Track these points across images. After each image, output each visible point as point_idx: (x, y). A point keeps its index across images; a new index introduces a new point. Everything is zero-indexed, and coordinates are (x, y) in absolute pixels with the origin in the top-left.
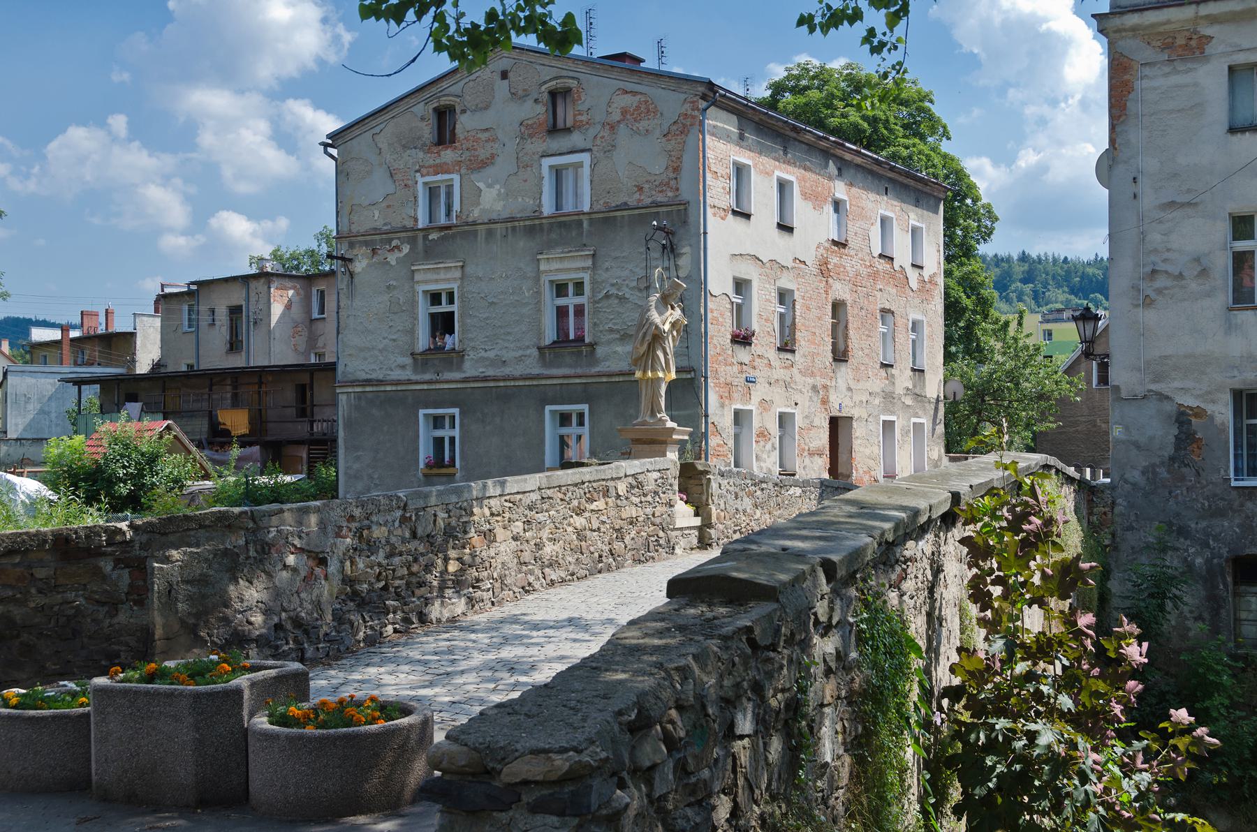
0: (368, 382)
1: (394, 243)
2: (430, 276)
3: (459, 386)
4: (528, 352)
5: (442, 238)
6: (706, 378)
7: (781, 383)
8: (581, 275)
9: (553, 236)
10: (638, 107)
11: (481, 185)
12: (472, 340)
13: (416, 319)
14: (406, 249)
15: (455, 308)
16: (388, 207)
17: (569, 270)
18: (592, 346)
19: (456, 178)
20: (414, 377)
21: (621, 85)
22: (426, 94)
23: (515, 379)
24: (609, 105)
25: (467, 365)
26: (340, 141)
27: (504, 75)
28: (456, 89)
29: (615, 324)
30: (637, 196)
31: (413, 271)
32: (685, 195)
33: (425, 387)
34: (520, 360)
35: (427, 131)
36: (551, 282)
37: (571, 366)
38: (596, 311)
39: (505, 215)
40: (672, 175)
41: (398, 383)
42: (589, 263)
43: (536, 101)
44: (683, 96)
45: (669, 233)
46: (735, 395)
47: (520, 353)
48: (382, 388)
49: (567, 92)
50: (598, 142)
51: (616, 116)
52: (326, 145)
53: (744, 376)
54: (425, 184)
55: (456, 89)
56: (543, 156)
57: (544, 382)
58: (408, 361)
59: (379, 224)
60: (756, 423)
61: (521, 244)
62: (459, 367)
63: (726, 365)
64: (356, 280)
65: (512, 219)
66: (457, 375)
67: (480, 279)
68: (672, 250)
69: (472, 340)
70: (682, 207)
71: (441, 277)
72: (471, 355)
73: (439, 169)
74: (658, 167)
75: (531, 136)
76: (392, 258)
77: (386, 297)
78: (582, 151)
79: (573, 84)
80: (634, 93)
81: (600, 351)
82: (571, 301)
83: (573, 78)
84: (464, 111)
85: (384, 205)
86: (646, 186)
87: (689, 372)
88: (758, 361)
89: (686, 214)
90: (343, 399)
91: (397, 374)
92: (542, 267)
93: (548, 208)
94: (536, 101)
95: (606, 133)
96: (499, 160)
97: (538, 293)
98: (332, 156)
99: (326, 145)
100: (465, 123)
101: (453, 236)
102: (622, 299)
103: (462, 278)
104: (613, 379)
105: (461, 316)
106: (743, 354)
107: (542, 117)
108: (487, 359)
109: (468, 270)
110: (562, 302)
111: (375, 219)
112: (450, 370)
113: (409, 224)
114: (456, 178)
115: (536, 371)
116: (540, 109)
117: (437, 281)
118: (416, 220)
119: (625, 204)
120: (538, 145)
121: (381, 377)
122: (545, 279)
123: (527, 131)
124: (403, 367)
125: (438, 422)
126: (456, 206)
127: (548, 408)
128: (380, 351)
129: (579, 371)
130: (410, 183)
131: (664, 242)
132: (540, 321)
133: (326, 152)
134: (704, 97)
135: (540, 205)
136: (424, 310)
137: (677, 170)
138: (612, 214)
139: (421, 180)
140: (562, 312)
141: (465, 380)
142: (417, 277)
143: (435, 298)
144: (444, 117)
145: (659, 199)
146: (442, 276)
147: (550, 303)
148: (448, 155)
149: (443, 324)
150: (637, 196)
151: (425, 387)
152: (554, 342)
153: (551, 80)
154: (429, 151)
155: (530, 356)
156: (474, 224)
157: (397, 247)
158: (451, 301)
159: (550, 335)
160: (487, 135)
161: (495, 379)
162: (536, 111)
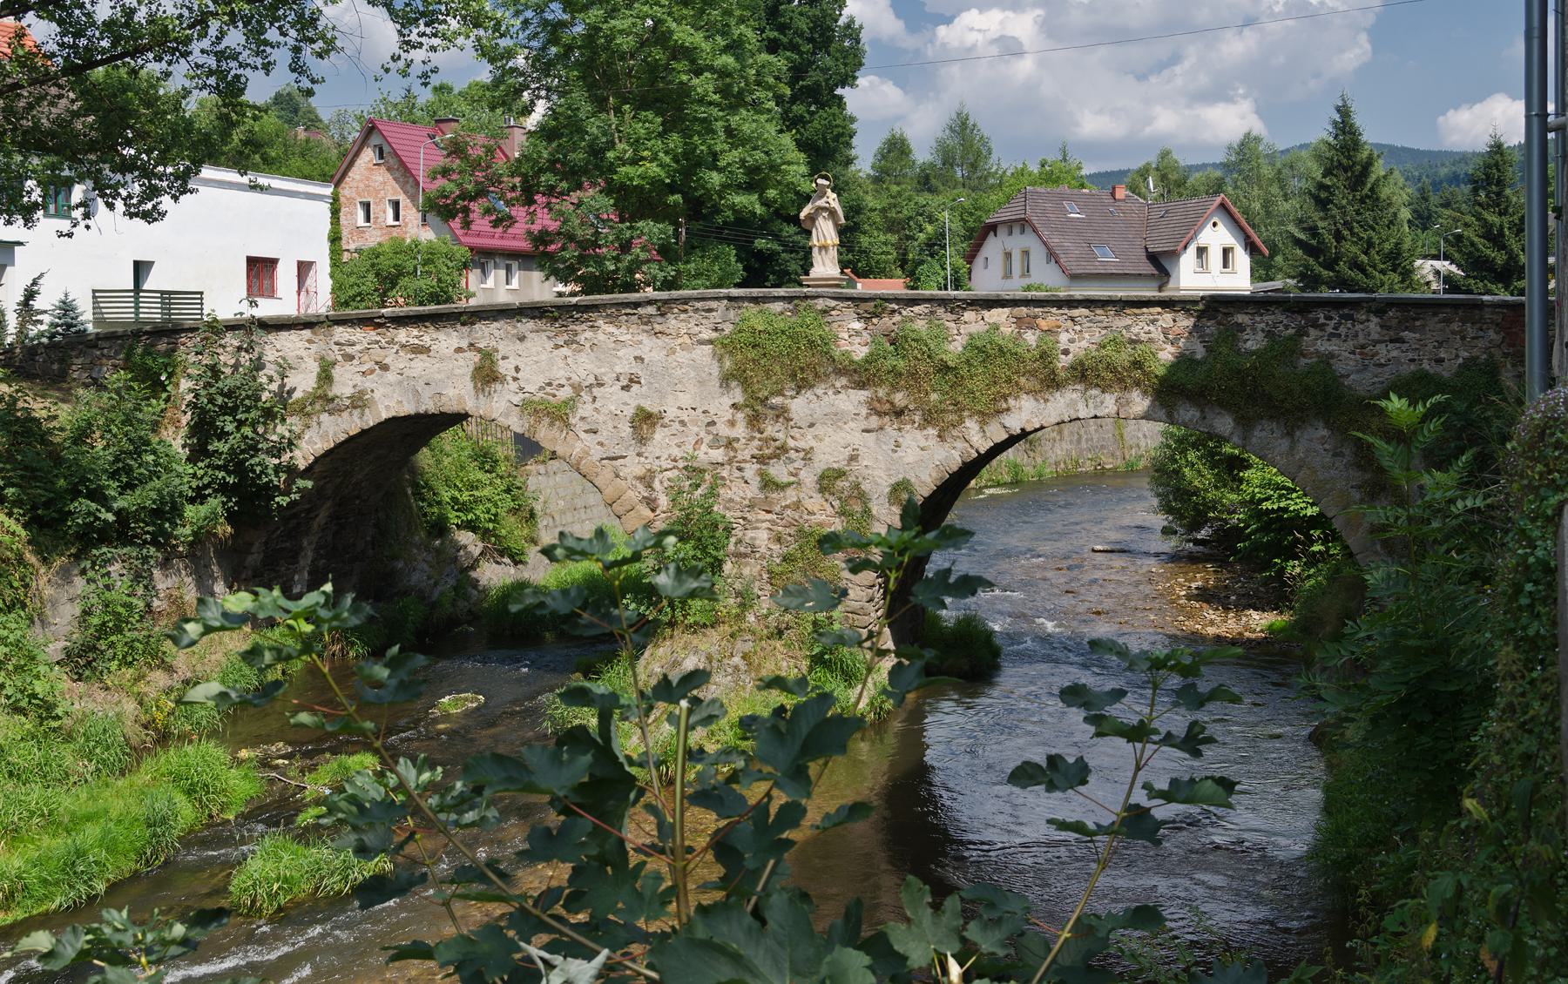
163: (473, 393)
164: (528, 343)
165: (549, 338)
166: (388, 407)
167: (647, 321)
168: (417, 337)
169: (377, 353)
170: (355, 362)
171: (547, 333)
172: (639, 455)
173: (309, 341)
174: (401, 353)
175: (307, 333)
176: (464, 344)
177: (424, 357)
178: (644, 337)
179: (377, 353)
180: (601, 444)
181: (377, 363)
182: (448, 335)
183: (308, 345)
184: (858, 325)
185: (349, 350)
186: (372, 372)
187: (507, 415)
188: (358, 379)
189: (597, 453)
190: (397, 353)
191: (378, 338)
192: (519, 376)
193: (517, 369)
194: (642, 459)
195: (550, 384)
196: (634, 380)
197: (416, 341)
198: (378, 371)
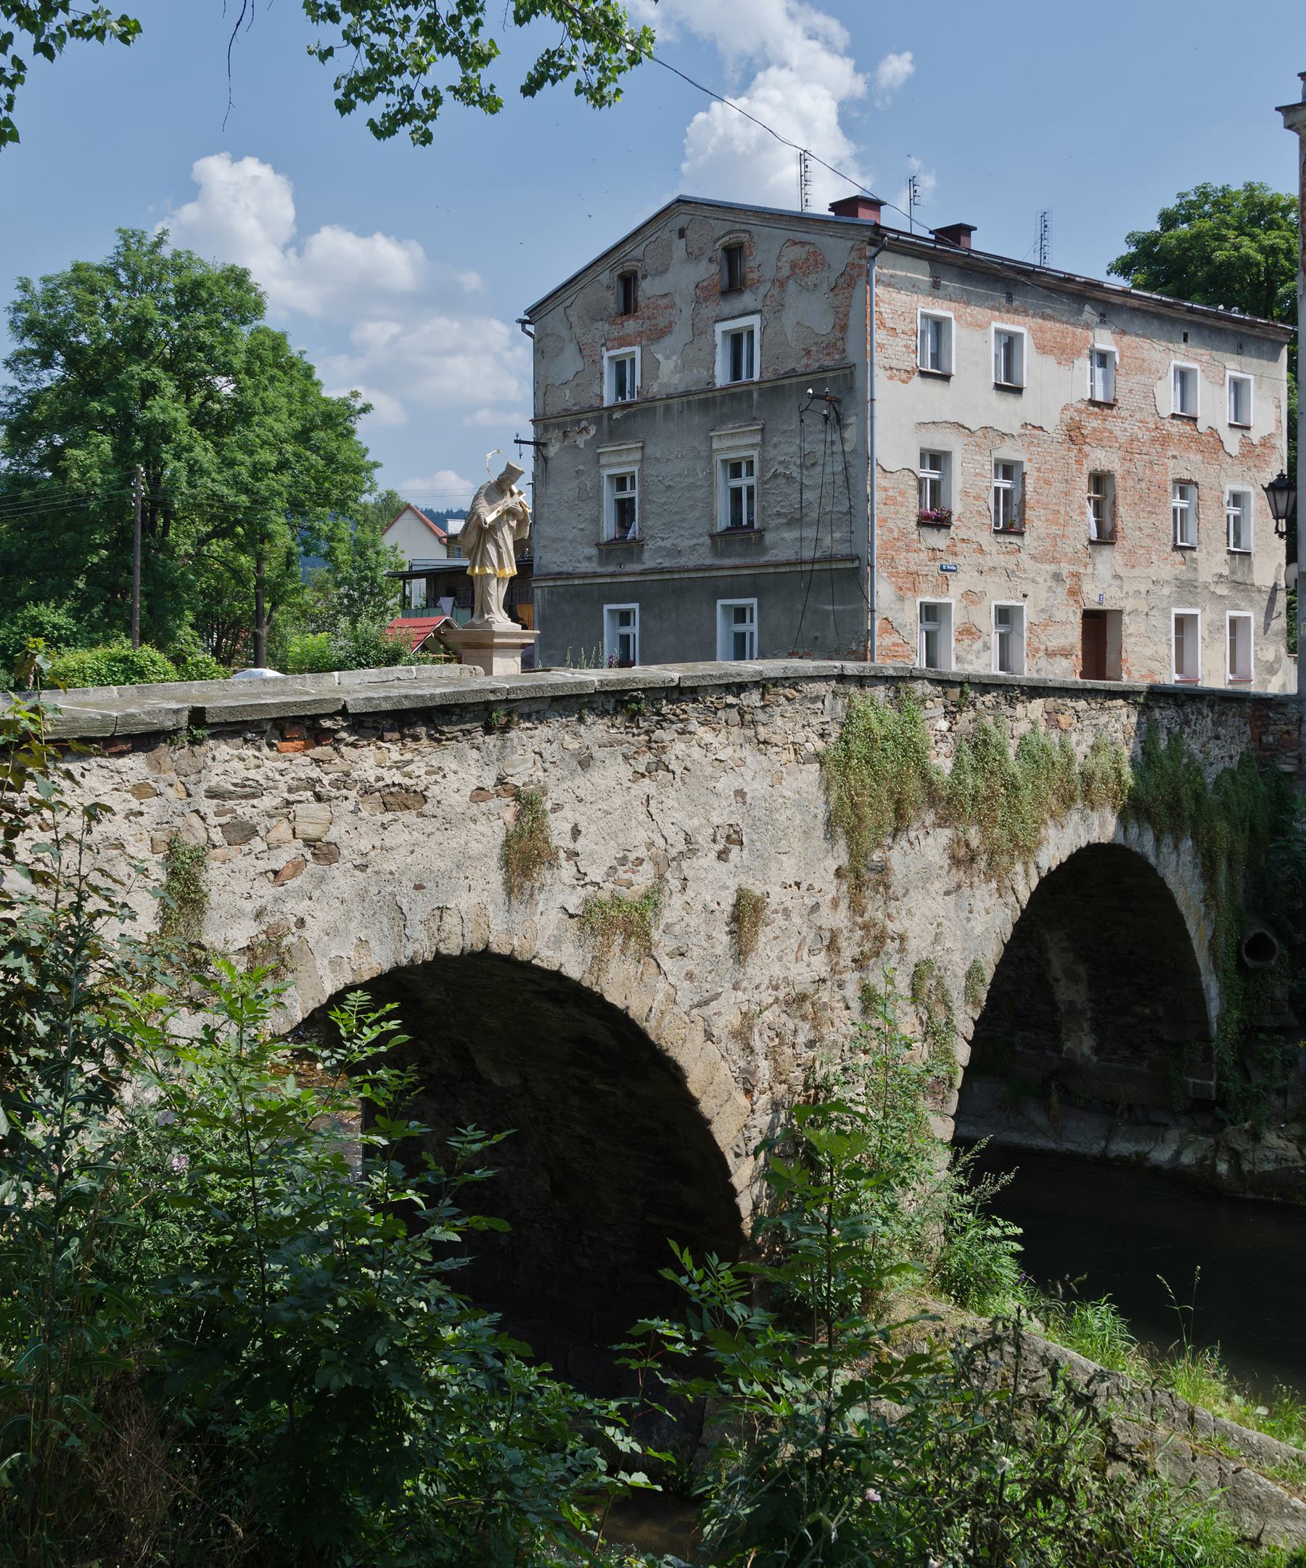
0: (559, 576)
1: (584, 424)
2: (615, 459)
3: (639, 578)
4: (701, 540)
5: (625, 417)
6: (872, 567)
7: (999, 571)
8: (751, 453)
9: (726, 410)
10: (807, 259)
11: (660, 357)
12: (650, 528)
13: (601, 506)
14: (593, 430)
15: (636, 494)
16: (578, 385)
17: (738, 447)
18: (761, 532)
19: (637, 349)
20: (600, 570)
21: (791, 235)
22: (612, 261)
23: (688, 571)
24: (779, 258)
25: (646, 556)
26: (536, 318)
27: (682, 234)
28: (638, 253)
29: (782, 507)
30: (805, 361)
31: (599, 454)
32: (852, 357)
33: (608, 580)
34: (693, 548)
35: (612, 300)
36: (725, 462)
37: (741, 556)
38: (764, 494)
39: (681, 389)
40: (839, 335)
41: (585, 576)
42: (758, 439)
43: (711, 260)
44: (850, 244)
45: (834, 402)
46: (923, 586)
47: (694, 541)
48: (571, 582)
49: (740, 247)
50: (768, 302)
51: (786, 271)
52: (523, 322)
53: (938, 564)
54: (611, 358)
55: (638, 253)
56: (717, 321)
57: (715, 574)
58: (593, 551)
59: (569, 405)
60: (957, 618)
61: (696, 420)
62: (639, 560)
63: (908, 551)
64: (549, 466)
65: (687, 393)
66: (637, 567)
67: (658, 460)
68: (839, 420)
69: (650, 528)
70: (847, 371)
71: (621, 461)
72: (650, 545)
73: (623, 342)
74: (824, 325)
75: (706, 299)
76: (581, 441)
77: (575, 484)
78: (753, 313)
79: (744, 237)
80: (803, 244)
81: (769, 538)
82: (743, 482)
83: (744, 231)
84: (645, 277)
85: (574, 383)
86: (814, 349)
87: (852, 560)
88: (960, 547)
89: (852, 380)
90: (538, 593)
91: (585, 567)
92: (715, 446)
93: (722, 376)
94: (711, 260)
95: (775, 292)
96: (676, 328)
97: (711, 474)
98: (529, 334)
99: (523, 322)
100: (647, 289)
101: (635, 414)
102: (789, 478)
103: (642, 461)
104: (780, 570)
105: (641, 501)
106: (936, 539)
107: (717, 278)
108: (664, 548)
109: (648, 451)
110: (735, 483)
111: (566, 399)
112: (632, 562)
113: (596, 403)
114: (637, 349)
115: (708, 561)
116: (714, 268)
117: (619, 464)
118: (602, 399)
120: (710, 310)
121: (570, 570)
122: (718, 458)
123: (702, 294)
124: (589, 559)
125: (625, 618)
126: (638, 382)
127: (720, 602)
128: (570, 542)
129: (749, 561)
130: (597, 358)
131: (825, 412)
132: (712, 505)
133: (524, 329)
134: (872, 243)
135: (713, 376)
136: (609, 496)
137: (844, 328)
138: (780, 383)
139: (606, 355)
140: (736, 493)
141: (643, 573)
142: (603, 461)
143: (620, 482)
144: (628, 282)
145: (826, 363)
146: (624, 458)
147: (723, 485)
148: (631, 326)
149: (625, 510)
150: (805, 361)
151: (608, 580)
152: (728, 529)
153: (724, 235)
154: (614, 323)
155: (702, 545)
156: (654, 399)
157: (585, 429)
158: (633, 487)
159: (723, 520)
160: (665, 301)
161: (671, 571)
162: (708, 271)
163: (501, 896)
164: (595, 775)
165: (626, 757)
166: (336, 963)
167: (746, 719)
168: (399, 766)
169: (311, 816)
170: (257, 844)
171: (624, 748)
172: (736, 987)
173: (141, 791)
174: (364, 814)
175: (135, 765)
176: (489, 782)
177: (408, 817)
178: (748, 752)
179: (311, 816)
180: (690, 976)
181: (309, 843)
182: (460, 757)
183: (135, 804)
184: (943, 725)
185: (244, 810)
186: (297, 867)
187: (557, 943)
188: (267, 891)
189: (686, 994)
190: (356, 811)
191: (315, 773)
192: (578, 846)
193: (576, 832)
194: (740, 993)
195: (623, 861)
196: (735, 839)
197: (398, 779)
198: (312, 866)
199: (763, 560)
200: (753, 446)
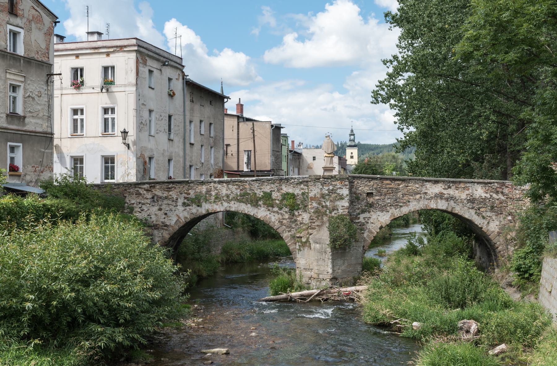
36: (11, 85)
37: (17, 125)
51: (31, 18)
81: (27, 120)
102: (33, 98)
104: (31, 134)
115: (5, 125)
119: (33, 57)
127: (9, 143)
129: (20, 128)
199: (25, 128)
200: (22, 82)
